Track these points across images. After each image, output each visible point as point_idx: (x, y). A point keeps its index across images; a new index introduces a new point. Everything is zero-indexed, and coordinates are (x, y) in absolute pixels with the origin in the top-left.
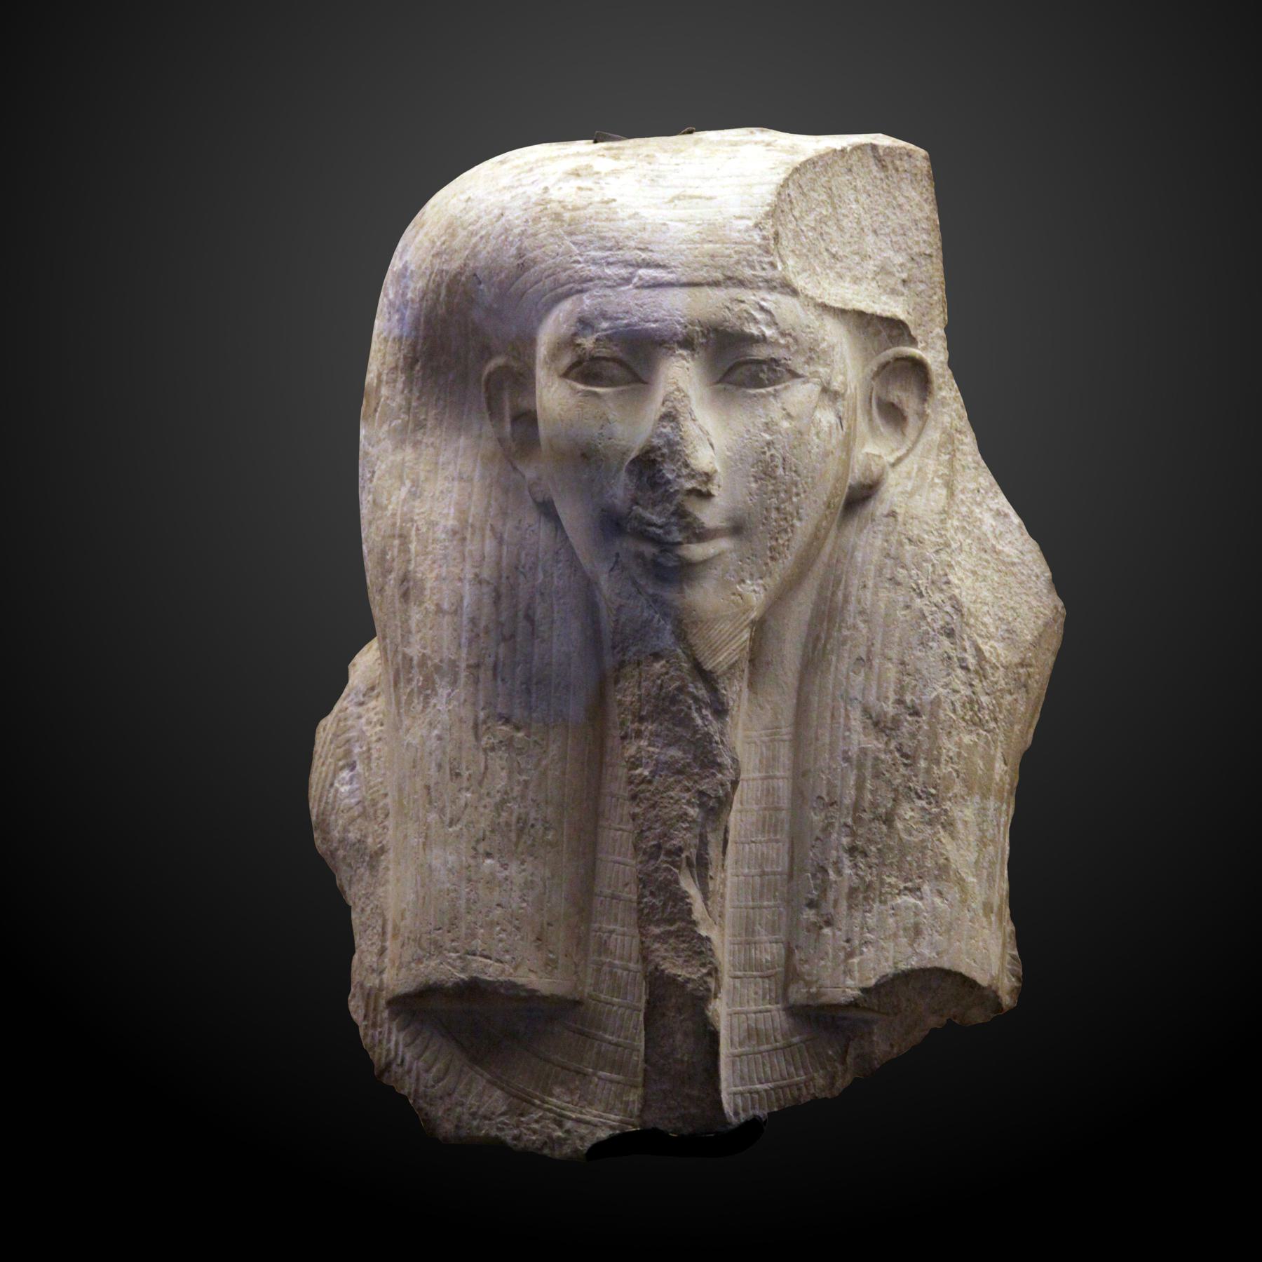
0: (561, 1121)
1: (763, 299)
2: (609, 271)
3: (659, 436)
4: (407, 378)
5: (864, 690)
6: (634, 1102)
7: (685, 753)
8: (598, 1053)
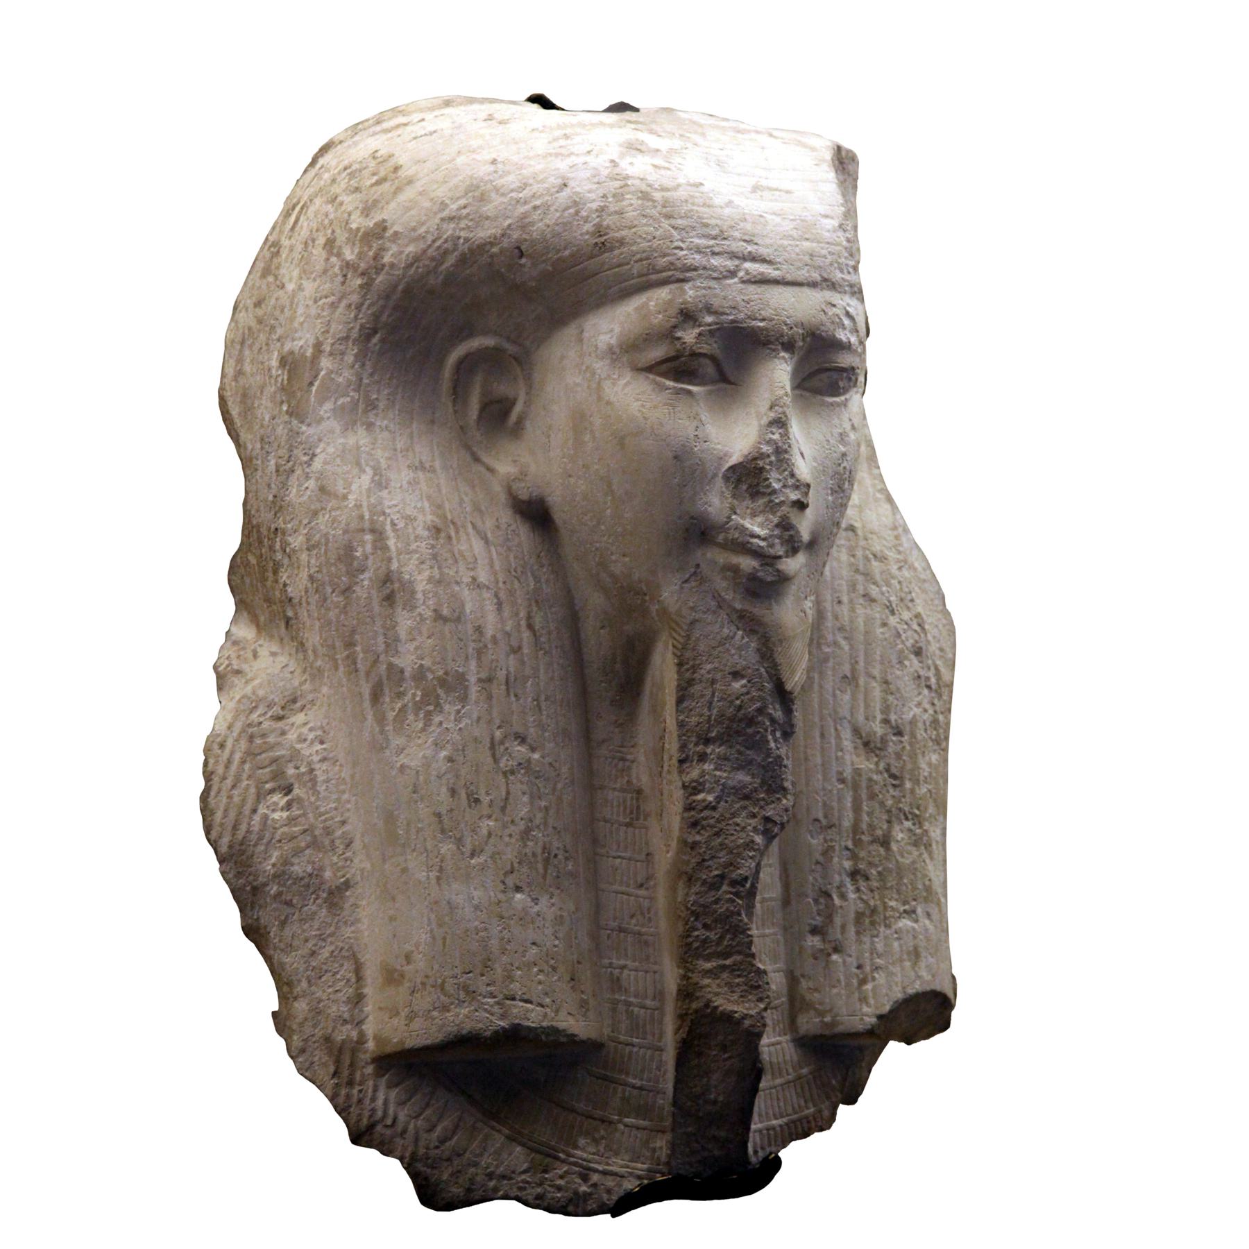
0: (587, 1175)
1: (848, 305)
2: (715, 261)
3: (769, 442)
4: (360, 350)
5: (853, 710)
6: (661, 1148)
7: (753, 778)
8: (623, 1099)
